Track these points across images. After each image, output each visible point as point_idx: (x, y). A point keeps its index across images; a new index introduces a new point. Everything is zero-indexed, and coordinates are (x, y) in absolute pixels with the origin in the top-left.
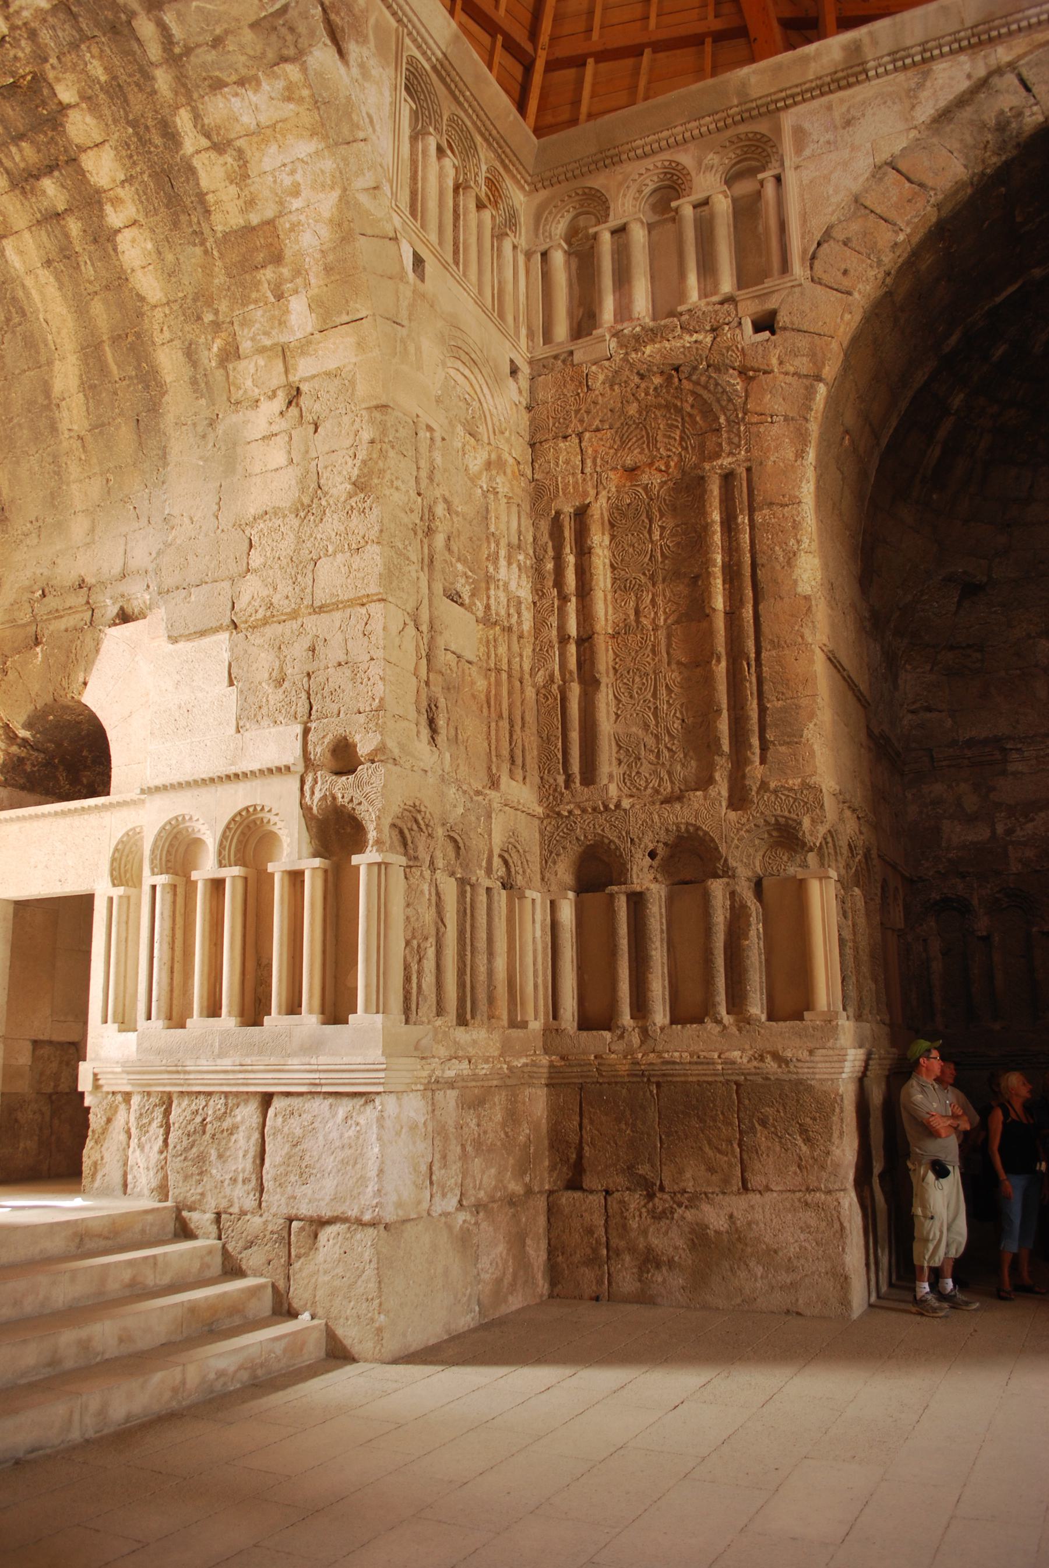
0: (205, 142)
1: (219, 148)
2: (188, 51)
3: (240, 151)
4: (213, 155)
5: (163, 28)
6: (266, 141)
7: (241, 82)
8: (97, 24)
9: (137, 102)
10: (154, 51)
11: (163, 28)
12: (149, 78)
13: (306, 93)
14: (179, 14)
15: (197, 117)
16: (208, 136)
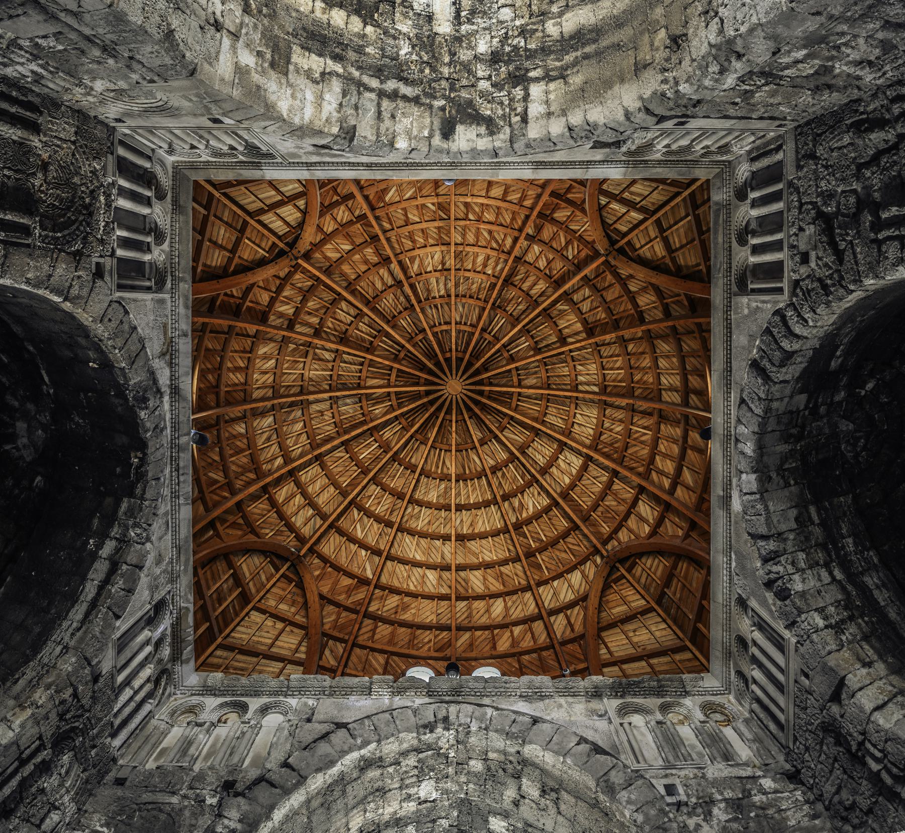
0: (328, 70)
1: (323, 74)
2: (359, 93)
3: (318, 83)
4: (321, 70)
5: (371, 90)
6: (316, 98)
7: (341, 105)
8: (385, 65)
9: (351, 55)
10: (366, 79)
11: (371, 90)
12: (359, 68)
13: (326, 130)
14: (372, 100)
15: (338, 75)
16: (329, 73)
